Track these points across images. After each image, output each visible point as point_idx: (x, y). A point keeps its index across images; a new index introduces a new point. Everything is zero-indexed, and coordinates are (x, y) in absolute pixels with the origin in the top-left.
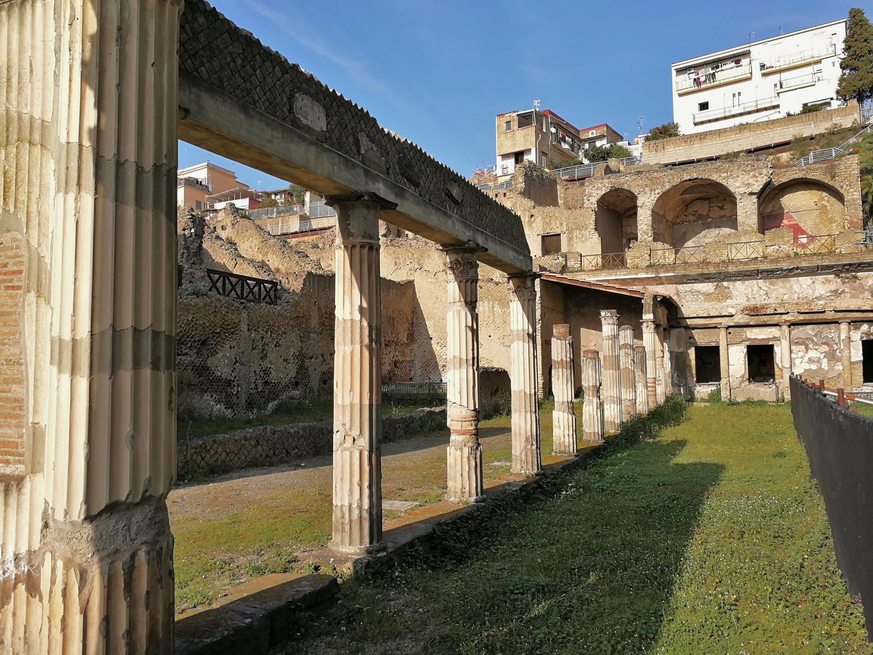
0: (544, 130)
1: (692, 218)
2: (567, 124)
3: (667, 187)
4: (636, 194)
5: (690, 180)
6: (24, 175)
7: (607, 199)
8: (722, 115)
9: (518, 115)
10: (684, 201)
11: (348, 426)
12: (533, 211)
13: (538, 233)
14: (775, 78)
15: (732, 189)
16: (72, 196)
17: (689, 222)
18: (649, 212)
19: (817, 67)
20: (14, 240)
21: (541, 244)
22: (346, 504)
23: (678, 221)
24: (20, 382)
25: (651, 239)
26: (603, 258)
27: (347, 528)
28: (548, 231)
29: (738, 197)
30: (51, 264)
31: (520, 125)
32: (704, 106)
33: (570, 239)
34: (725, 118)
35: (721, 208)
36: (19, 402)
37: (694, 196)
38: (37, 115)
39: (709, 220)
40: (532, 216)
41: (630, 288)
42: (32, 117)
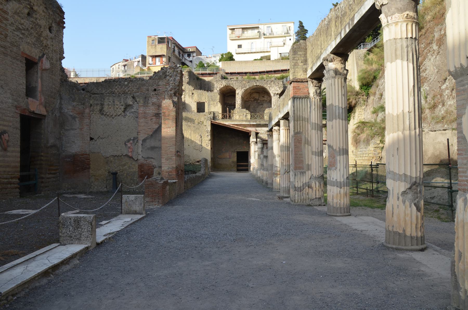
0: (170, 46)
1: (252, 100)
2: (179, 44)
3: (248, 88)
4: (235, 89)
5: (256, 86)
6: (304, 126)
7: (223, 89)
8: (247, 52)
9: (158, 38)
10: (250, 92)
11: (287, 169)
12: (194, 92)
13: (195, 101)
14: (269, 40)
15: (271, 92)
16: (316, 131)
17: (251, 101)
18: (240, 97)
19: (284, 38)
20: (300, 136)
21: (196, 106)
22: (287, 186)
23: (247, 100)
24: (303, 157)
25: (241, 107)
26: (222, 115)
27: (287, 191)
28: (200, 100)
29: (272, 95)
30: (311, 140)
31: (159, 42)
32: (240, 46)
33: (209, 105)
34: (248, 53)
35: (263, 97)
36: (302, 161)
37: (254, 91)
38: (306, 117)
39: (259, 101)
40: (193, 94)
41: (245, 129)
42: (305, 117)
